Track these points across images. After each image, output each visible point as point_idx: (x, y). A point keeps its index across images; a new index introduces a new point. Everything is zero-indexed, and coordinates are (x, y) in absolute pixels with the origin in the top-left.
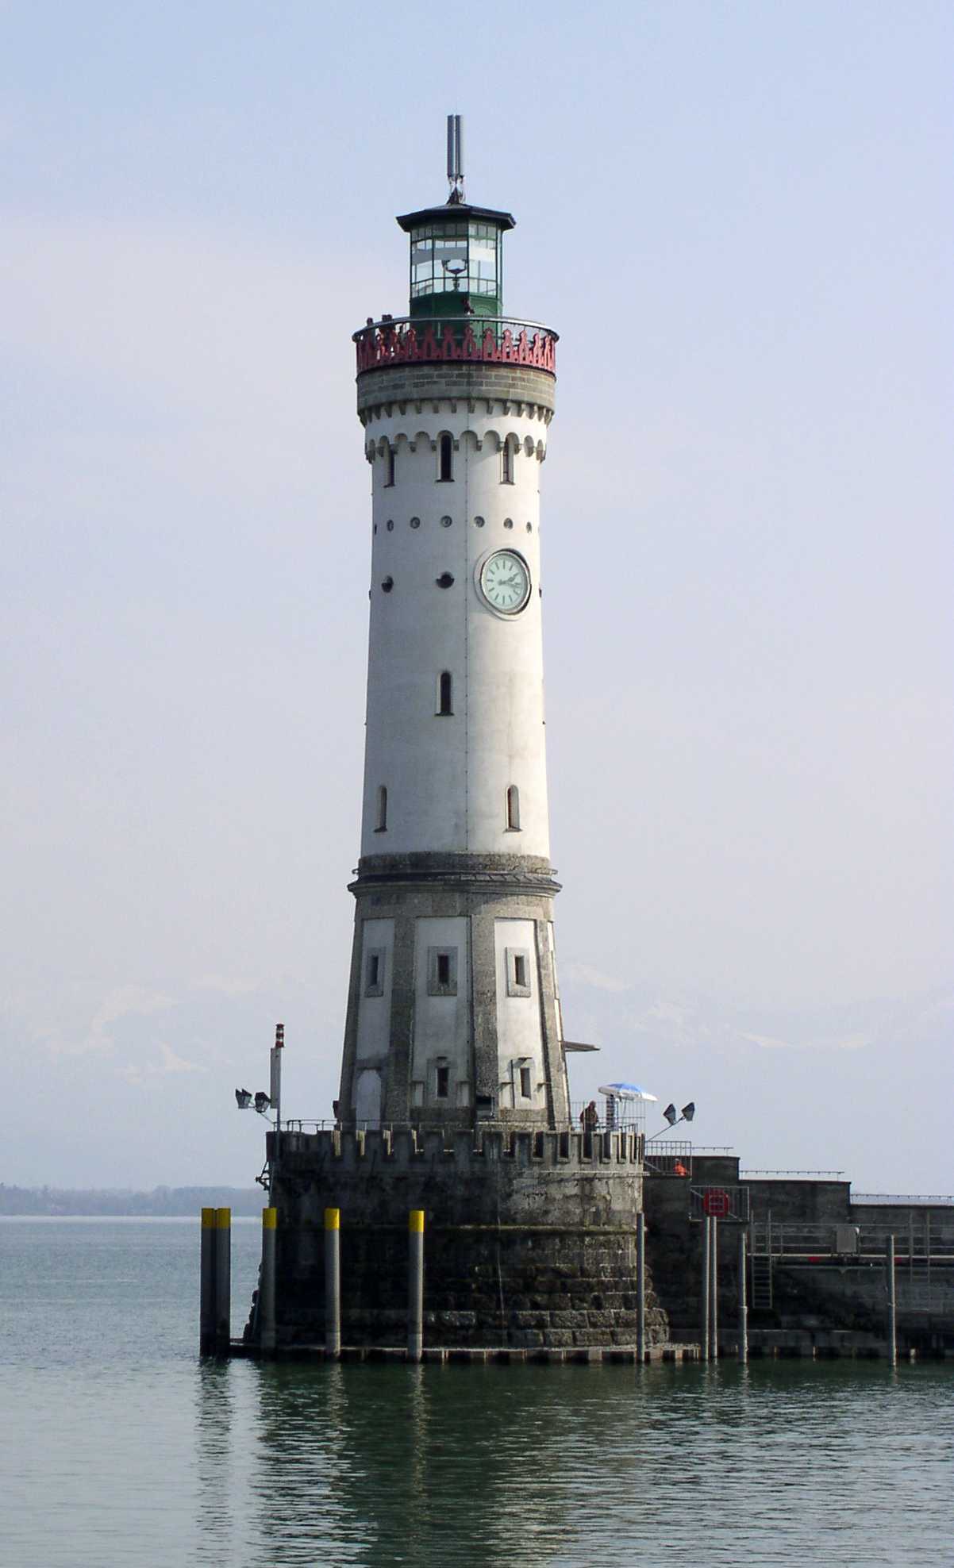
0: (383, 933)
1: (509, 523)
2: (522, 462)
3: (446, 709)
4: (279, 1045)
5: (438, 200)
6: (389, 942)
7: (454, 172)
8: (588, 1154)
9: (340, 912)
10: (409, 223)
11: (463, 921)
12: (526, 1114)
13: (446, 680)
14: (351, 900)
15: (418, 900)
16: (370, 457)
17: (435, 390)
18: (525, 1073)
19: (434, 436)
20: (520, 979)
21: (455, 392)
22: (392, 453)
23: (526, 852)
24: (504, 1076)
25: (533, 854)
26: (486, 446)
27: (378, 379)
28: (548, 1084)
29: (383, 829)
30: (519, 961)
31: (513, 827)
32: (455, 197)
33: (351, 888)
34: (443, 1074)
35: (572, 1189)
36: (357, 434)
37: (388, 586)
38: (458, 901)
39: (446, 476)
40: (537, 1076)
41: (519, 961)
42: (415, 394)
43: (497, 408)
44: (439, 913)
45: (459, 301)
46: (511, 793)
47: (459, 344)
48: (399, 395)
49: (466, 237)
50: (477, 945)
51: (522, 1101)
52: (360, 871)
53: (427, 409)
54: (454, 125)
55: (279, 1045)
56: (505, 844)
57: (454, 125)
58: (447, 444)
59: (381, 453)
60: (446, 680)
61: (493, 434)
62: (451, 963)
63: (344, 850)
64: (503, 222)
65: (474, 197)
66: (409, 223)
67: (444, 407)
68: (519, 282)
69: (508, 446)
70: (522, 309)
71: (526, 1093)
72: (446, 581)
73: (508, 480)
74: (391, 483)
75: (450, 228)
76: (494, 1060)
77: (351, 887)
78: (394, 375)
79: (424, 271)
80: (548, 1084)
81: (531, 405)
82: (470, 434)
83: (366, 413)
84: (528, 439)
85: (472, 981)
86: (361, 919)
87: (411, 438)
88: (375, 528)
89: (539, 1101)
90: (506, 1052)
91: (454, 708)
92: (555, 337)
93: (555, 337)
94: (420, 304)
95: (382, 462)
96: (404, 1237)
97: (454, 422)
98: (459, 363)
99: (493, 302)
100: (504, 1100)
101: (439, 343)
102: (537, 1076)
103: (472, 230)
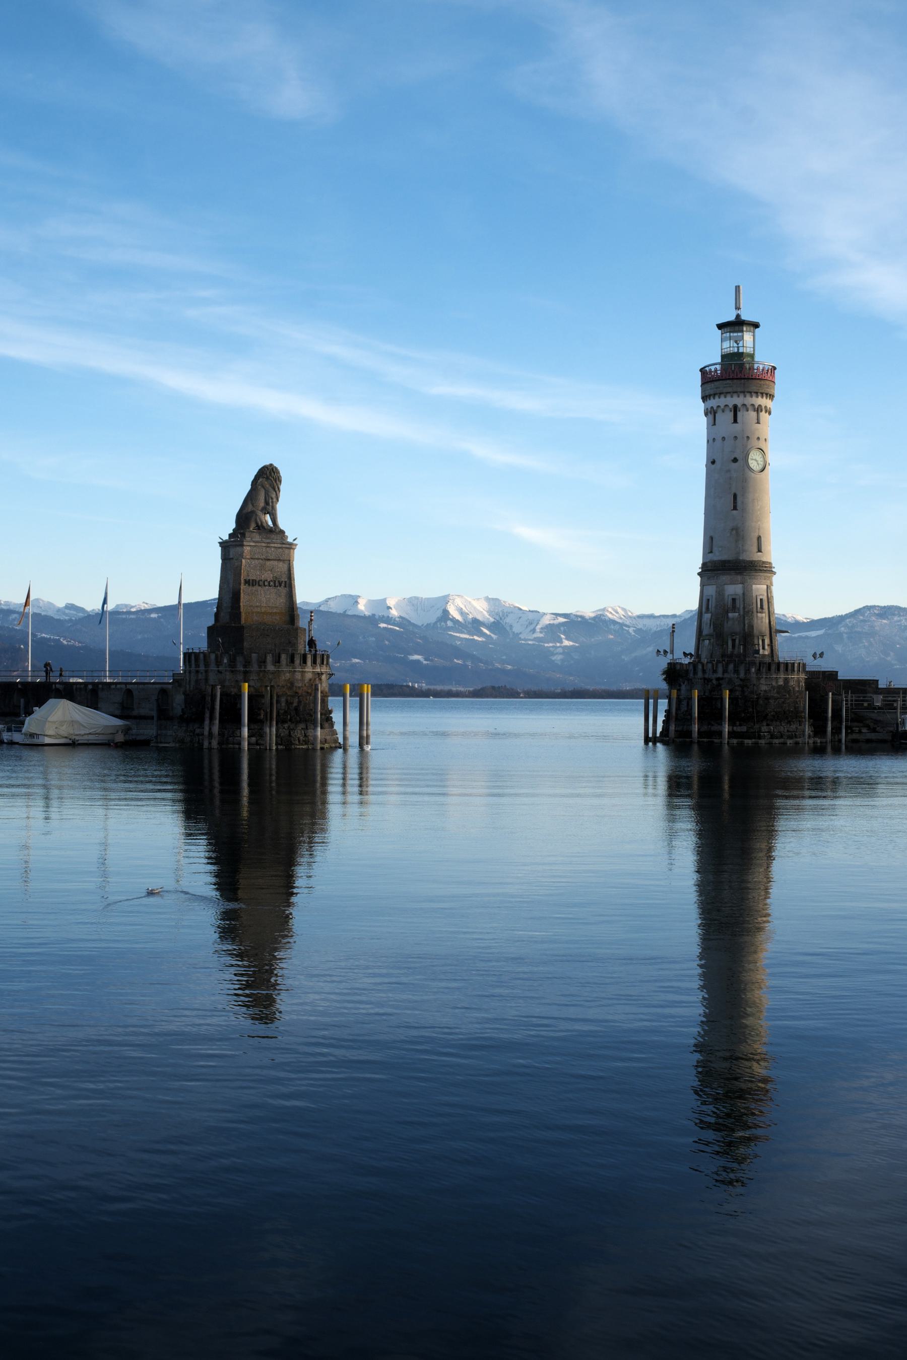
0: (711, 590)
1: (758, 438)
2: (763, 415)
3: (735, 508)
4: (673, 631)
5: (732, 317)
6: (714, 594)
7: (738, 308)
8: (787, 670)
9: (696, 582)
10: (720, 326)
11: (741, 586)
12: (764, 656)
13: (735, 496)
14: (699, 578)
15: (725, 578)
16: (706, 414)
17: (730, 390)
18: (763, 641)
19: (731, 406)
20: (762, 608)
21: (739, 390)
23: (764, 559)
24: (756, 642)
26: (750, 408)
27: (708, 386)
28: (771, 645)
29: (711, 552)
30: (761, 600)
31: (760, 550)
32: (738, 316)
33: (699, 574)
34: (733, 641)
35: (781, 683)
36: (701, 406)
37: (713, 462)
38: (739, 578)
39: (735, 421)
40: (767, 641)
41: (761, 600)
42: (725, 390)
43: (754, 395)
44: (733, 583)
45: (739, 355)
46: (759, 538)
47: (741, 372)
48: (718, 391)
49: (742, 331)
50: (746, 594)
52: (702, 568)
53: (729, 396)
54: (737, 288)
55: (673, 631)
56: (757, 557)
57: (737, 288)
58: (735, 409)
59: (711, 413)
61: (753, 405)
62: (737, 602)
63: (696, 558)
64: (756, 325)
65: (743, 317)
66: (720, 326)
67: (735, 396)
68: (762, 348)
70: (763, 359)
71: (764, 648)
72: (735, 460)
74: (714, 424)
77: (699, 574)
78: (717, 383)
79: (726, 344)
80: (771, 645)
81: (767, 394)
82: (744, 405)
83: (704, 398)
84: (766, 407)
85: (744, 608)
86: (703, 585)
87: (722, 407)
88: (708, 441)
92: (775, 368)
93: (775, 368)
94: (724, 357)
95: (711, 416)
96: (722, 700)
97: (738, 400)
98: (741, 379)
99: (752, 356)
101: (733, 372)
103: (745, 329)
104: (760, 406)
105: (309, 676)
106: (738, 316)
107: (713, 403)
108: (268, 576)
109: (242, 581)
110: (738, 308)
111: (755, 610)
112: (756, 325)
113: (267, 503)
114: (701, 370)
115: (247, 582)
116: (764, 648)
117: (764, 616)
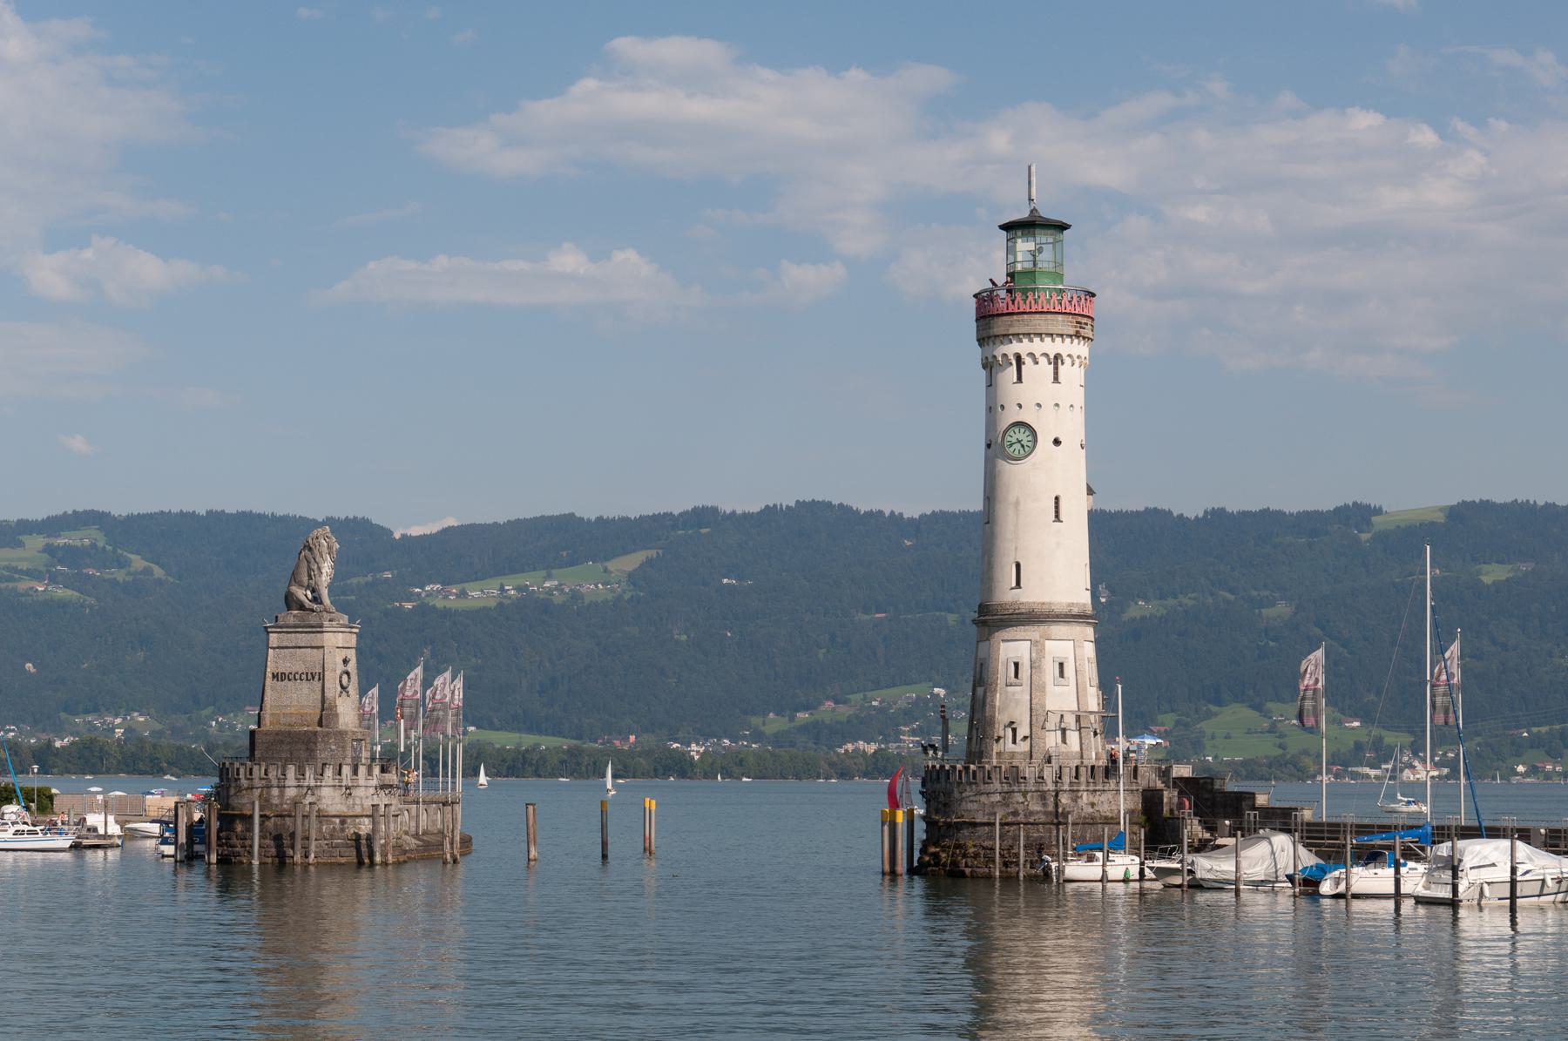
12: (1013, 755)
23: (1023, 600)
24: (999, 730)
25: (1031, 600)
30: (1016, 665)
32: (1033, 211)
41: (1016, 665)
46: (1018, 566)
51: (1010, 746)
61: (1005, 355)
71: (1014, 742)
73: (1020, 379)
76: (991, 722)
84: (1031, 355)
89: (1024, 747)
90: (1002, 718)
100: (996, 748)
102: (1023, 731)
105: (291, 792)
106: (1033, 211)
108: (299, 667)
109: (269, 675)
110: (1030, 200)
111: (1001, 682)
113: (310, 577)
115: (275, 676)
116: (1014, 742)
117: (1021, 693)
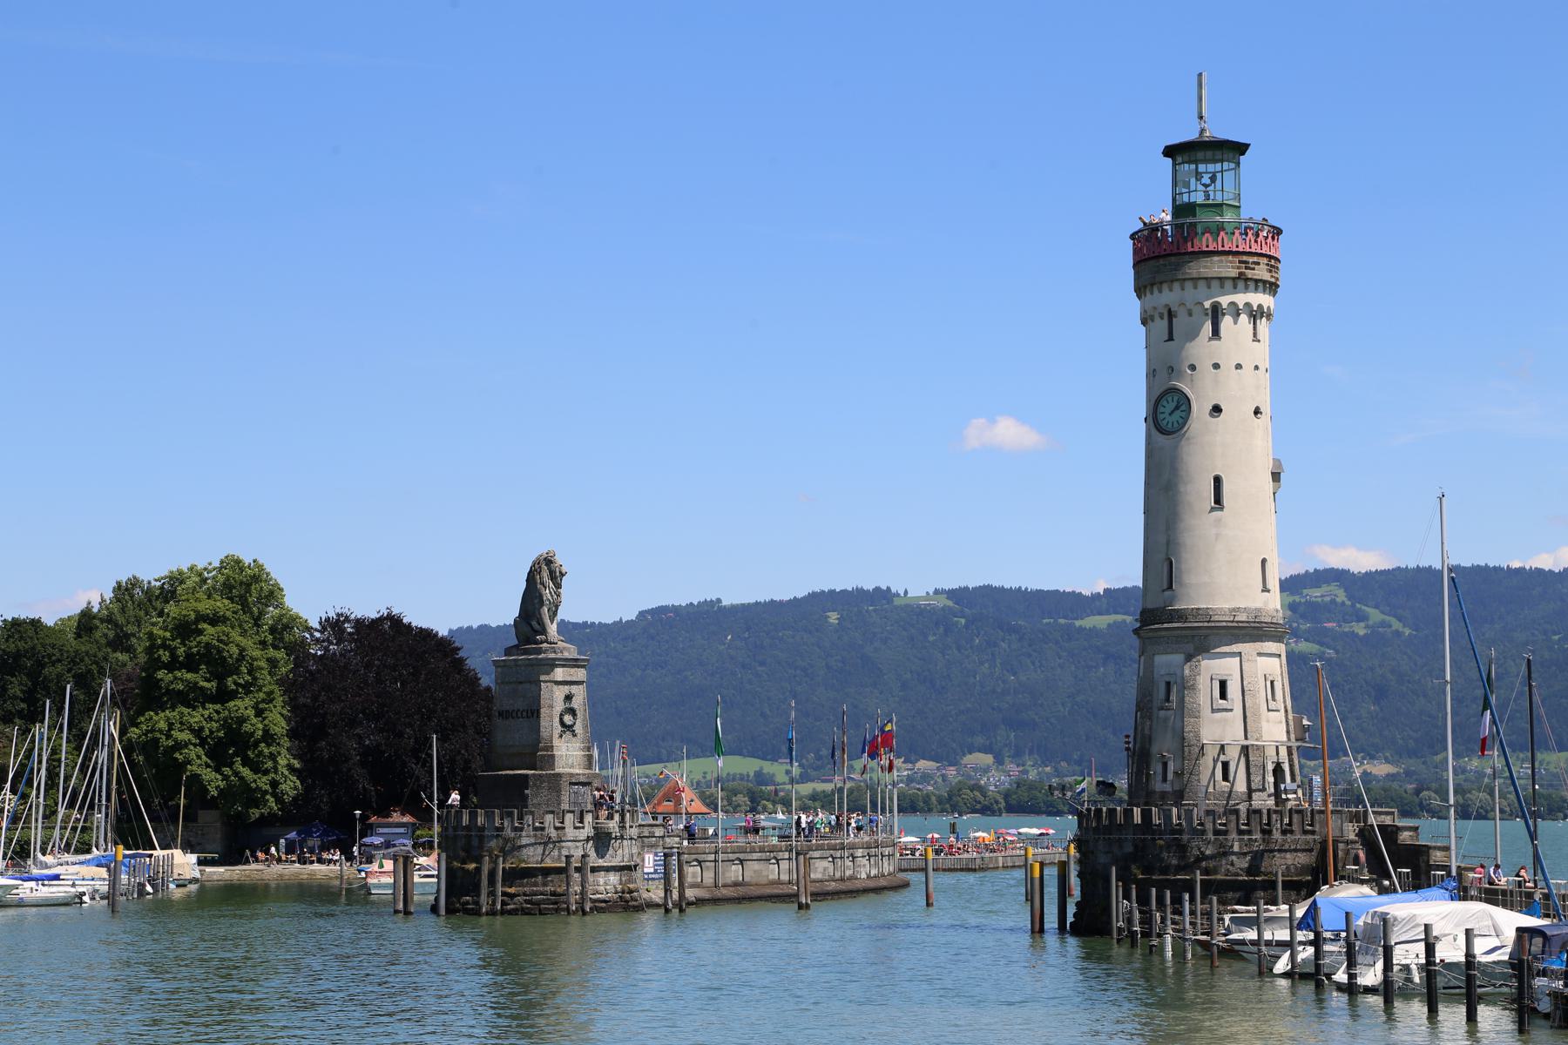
1: (1257, 368)
5: (1191, 135)
10: (1170, 151)
22: (1171, 315)
31: (1265, 590)
32: (1203, 131)
39: (1216, 333)
58: (1216, 313)
60: (1218, 481)
61: (1247, 305)
64: (1242, 148)
69: (1256, 314)
72: (1217, 409)
74: (1171, 338)
75: (1209, 154)
91: (1226, 500)
104: (1260, 306)
107: (1167, 297)
112: (1242, 148)
114: (1132, 237)
